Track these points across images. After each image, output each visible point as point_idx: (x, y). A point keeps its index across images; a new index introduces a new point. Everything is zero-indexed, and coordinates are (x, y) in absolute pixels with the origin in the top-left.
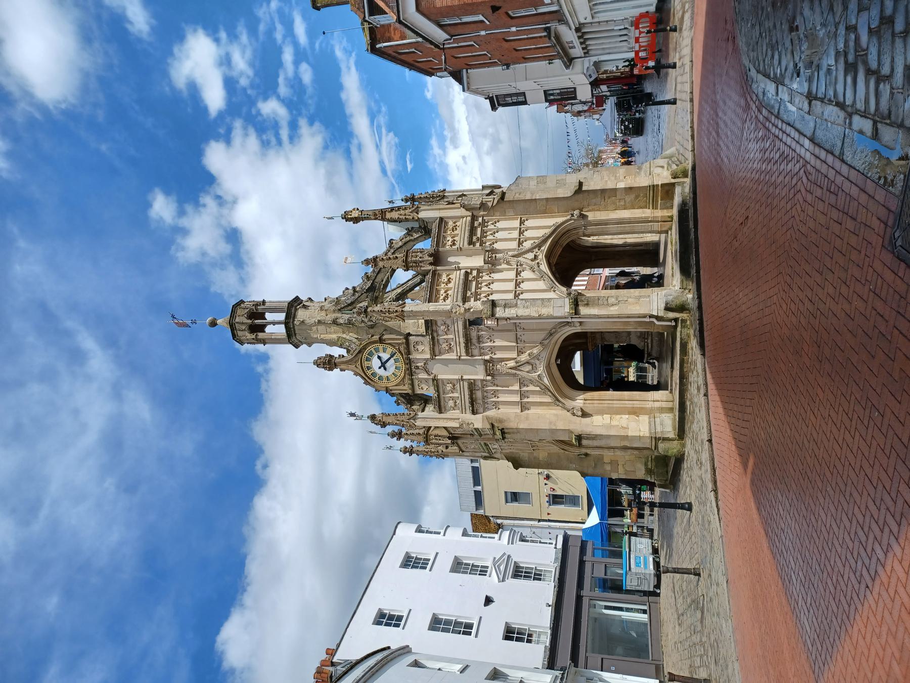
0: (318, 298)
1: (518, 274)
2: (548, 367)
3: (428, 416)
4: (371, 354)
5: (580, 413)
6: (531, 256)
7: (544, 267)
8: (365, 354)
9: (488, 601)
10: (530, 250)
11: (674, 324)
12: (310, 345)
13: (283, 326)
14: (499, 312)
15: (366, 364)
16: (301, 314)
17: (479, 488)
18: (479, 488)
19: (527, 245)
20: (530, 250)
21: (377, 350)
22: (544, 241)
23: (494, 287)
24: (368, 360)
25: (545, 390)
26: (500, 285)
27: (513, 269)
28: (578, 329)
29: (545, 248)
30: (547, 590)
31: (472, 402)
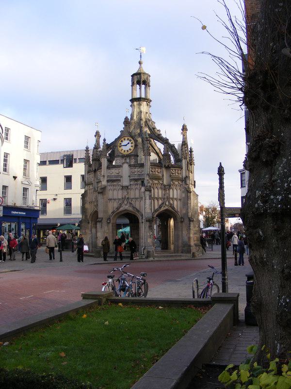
0: (151, 110)
1: (161, 198)
2: (126, 210)
3: (104, 162)
4: (130, 141)
5: (109, 222)
6: (167, 203)
7: (163, 209)
8: (130, 138)
9: (15, 178)
10: (169, 202)
11: (143, 253)
12: (131, 106)
13: (139, 97)
14: (147, 193)
15: (126, 138)
16: (145, 103)
17: (48, 163)
18: (48, 163)
19: (171, 202)
20: (169, 202)
21: (132, 143)
22: (173, 208)
23: (156, 190)
24: (128, 139)
25: (118, 209)
26: (158, 192)
27: (162, 196)
28: (140, 221)
29: (170, 209)
30: (19, 203)
31: (113, 181)
